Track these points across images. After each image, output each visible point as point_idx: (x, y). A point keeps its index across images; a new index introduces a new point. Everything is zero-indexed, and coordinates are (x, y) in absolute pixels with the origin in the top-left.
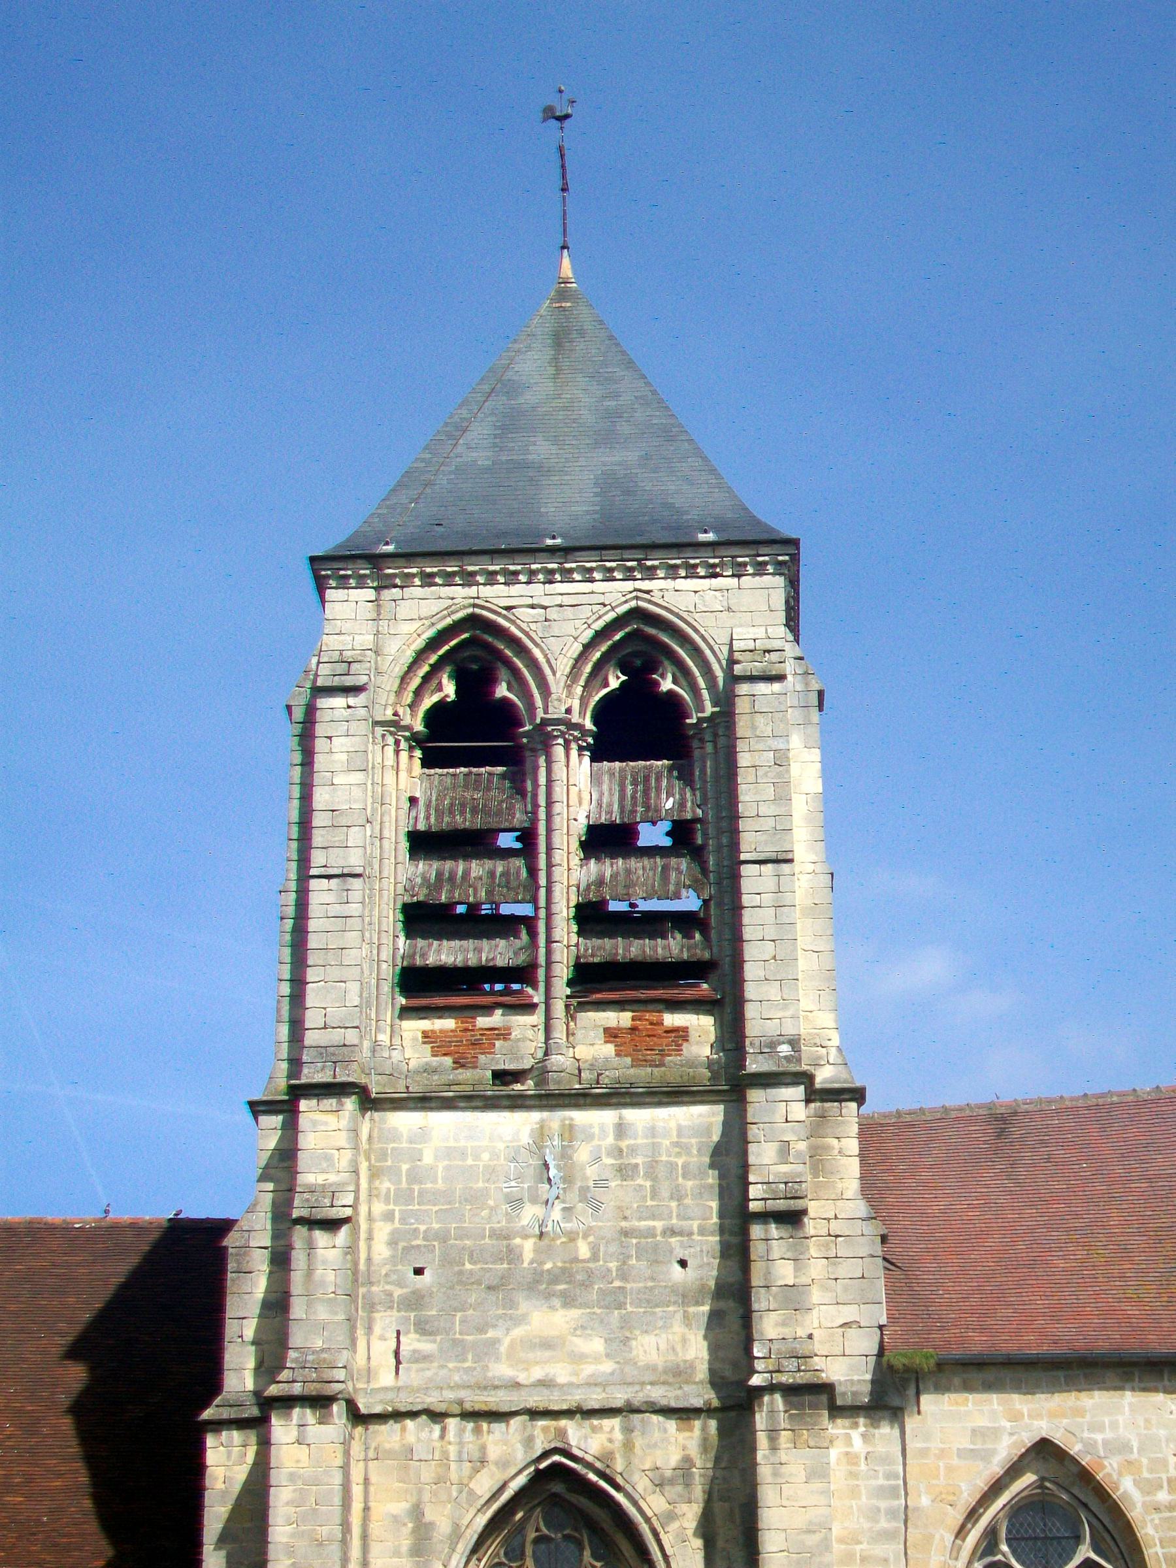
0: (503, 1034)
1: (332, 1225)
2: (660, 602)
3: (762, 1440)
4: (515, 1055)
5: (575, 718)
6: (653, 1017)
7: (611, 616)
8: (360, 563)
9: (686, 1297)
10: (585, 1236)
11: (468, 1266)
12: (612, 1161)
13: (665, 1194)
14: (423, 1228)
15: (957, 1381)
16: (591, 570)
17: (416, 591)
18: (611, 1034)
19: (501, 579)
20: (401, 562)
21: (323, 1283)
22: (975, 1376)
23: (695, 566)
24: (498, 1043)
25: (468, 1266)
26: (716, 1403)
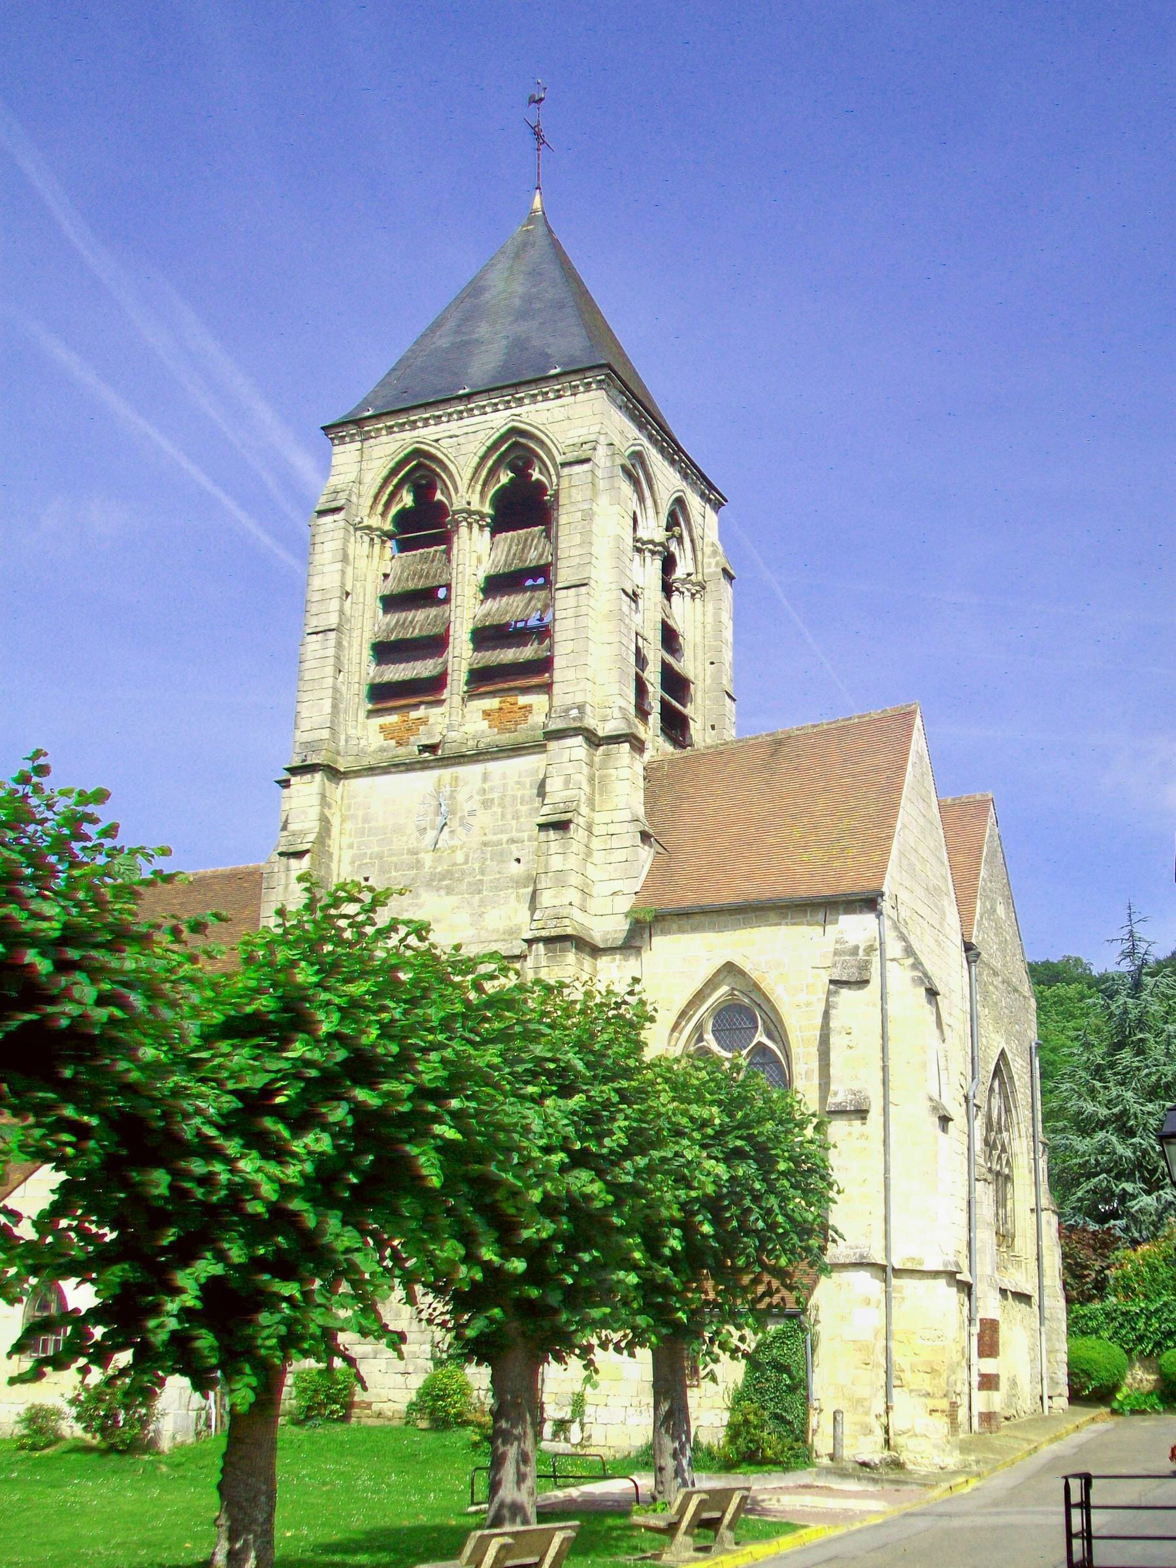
0: (423, 721)
2: (527, 421)
4: (430, 734)
5: (475, 506)
6: (511, 699)
7: (497, 435)
8: (351, 426)
10: (462, 848)
11: (394, 874)
12: (479, 798)
13: (509, 816)
14: (369, 852)
15: (675, 926)
16: (484, 407)
17: (384, 439)
18: (487, 714)
19: (432, 422)
20: (374, 421)
22: (684, 921)
23: (547, 393)
24: (421, 728)
25: (394, 874)
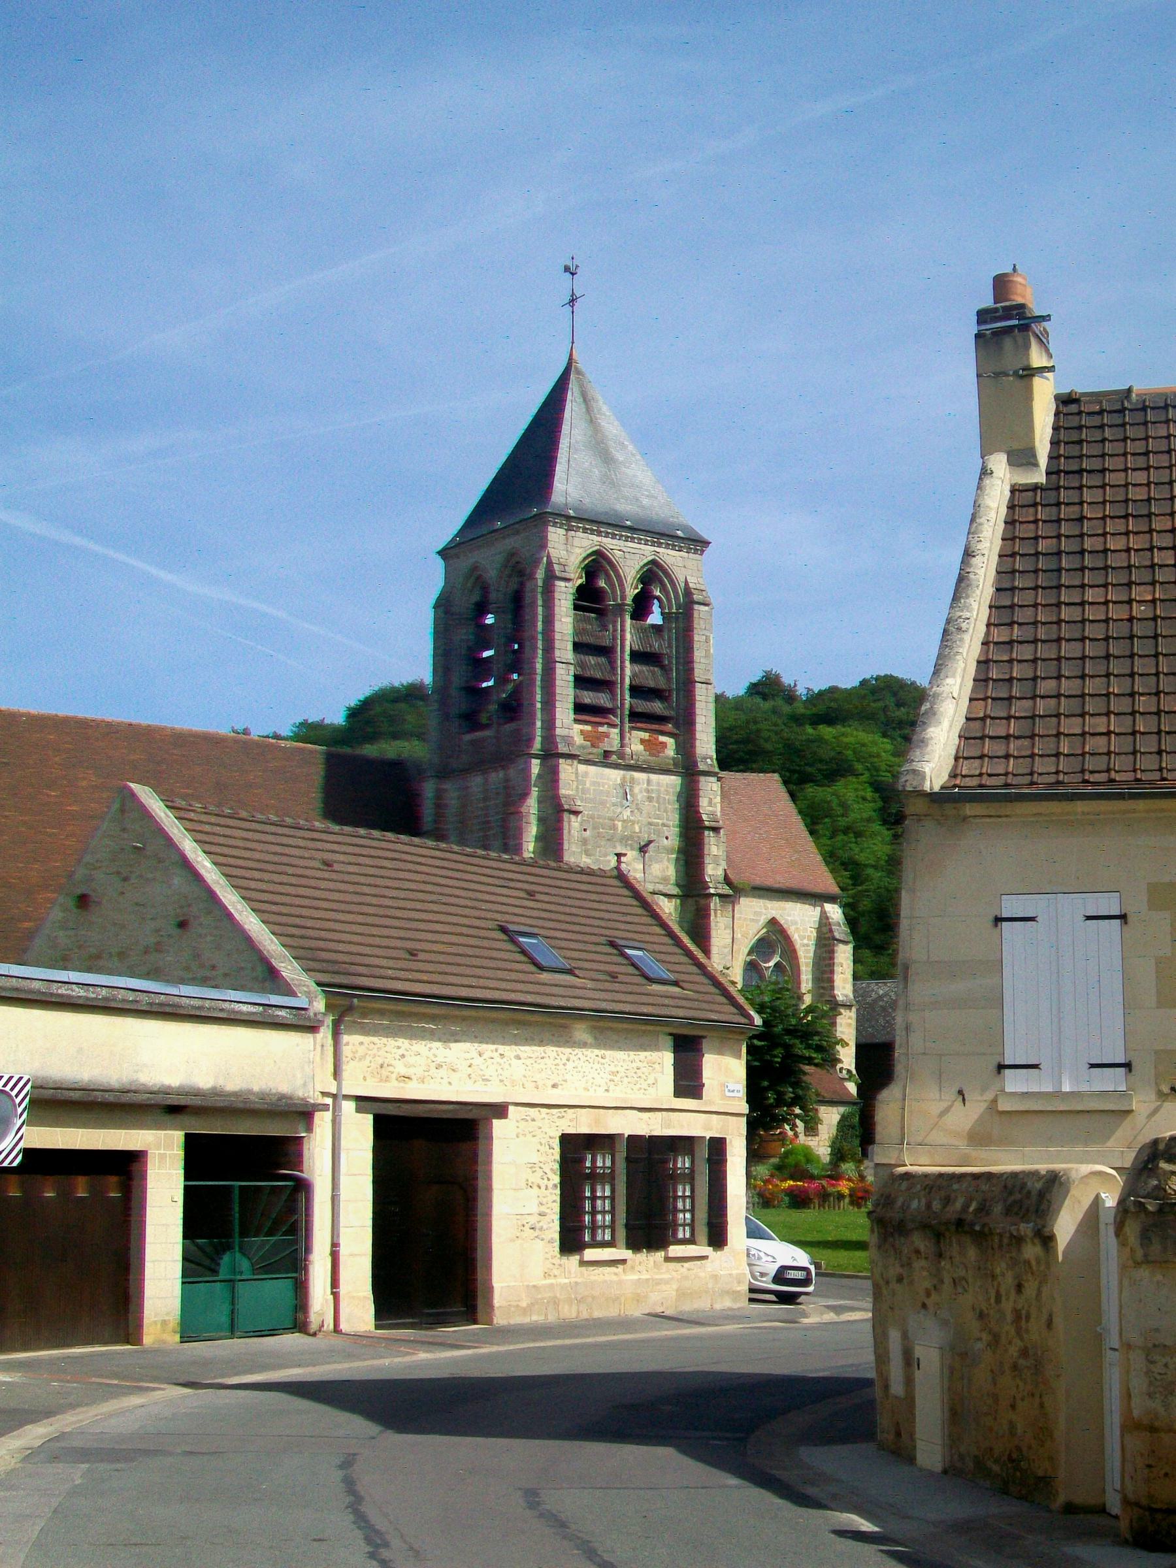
1: (576, 813)
3: (712, 912)
9: (669, 851)
17: (580, 534)
18: (642, 741)
21: (574, 837)
26: (680, 893)
